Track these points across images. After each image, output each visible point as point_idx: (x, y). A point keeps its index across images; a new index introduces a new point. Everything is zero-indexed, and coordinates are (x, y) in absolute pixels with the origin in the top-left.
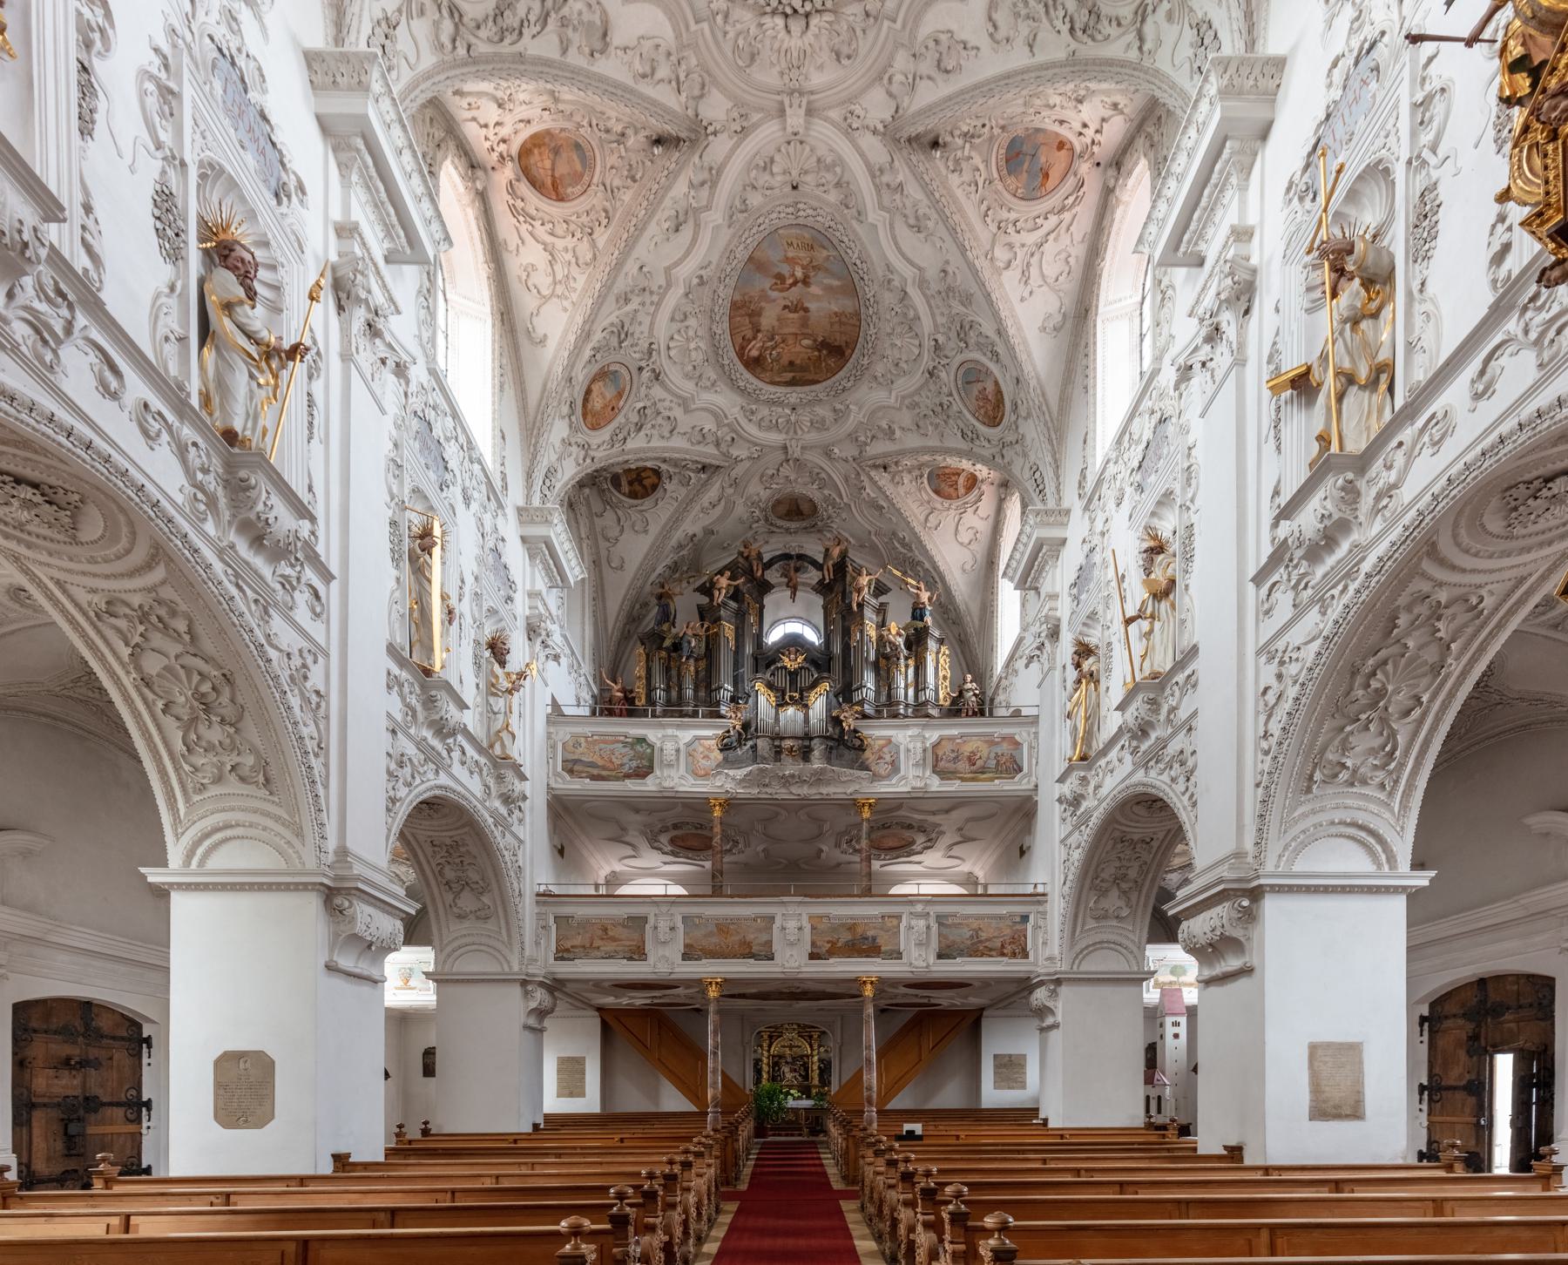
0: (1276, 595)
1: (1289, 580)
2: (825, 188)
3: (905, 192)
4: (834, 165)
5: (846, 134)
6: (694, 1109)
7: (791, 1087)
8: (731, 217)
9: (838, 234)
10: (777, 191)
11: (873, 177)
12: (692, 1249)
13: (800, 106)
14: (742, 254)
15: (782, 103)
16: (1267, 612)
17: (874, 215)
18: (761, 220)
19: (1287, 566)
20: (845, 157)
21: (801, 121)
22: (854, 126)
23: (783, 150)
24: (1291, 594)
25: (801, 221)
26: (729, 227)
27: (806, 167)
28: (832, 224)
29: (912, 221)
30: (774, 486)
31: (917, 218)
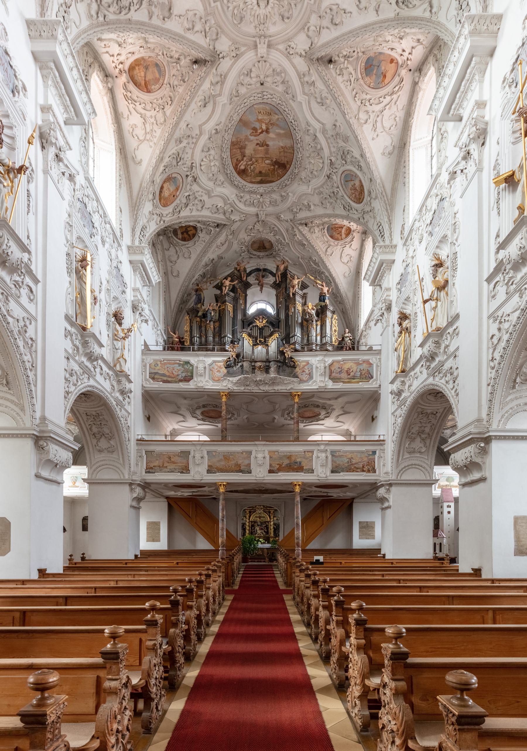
2: (276, 84)
3: (316, 86)
4: (281, 72)
5: (287, 57)
6: (212, 548)
7: (260, 537)
8: (231, 99)
9: (283, 107)
10: (253, 86)
11: (300, 78)
12: (210, 618)
13: (264, 43)
14: (236, 118)
15: (256, 42)
17: (300, 97)
18: (245, 101)
20: (288, 70)
21: (265, 51)
22: (291, 53)
23: (256, 65)
25: (265, 101)
26: (230, 104)
27: (267, 74)
28: (280, 102)
29: (319, 100)
30: (252, 234)
31: (322, 99)
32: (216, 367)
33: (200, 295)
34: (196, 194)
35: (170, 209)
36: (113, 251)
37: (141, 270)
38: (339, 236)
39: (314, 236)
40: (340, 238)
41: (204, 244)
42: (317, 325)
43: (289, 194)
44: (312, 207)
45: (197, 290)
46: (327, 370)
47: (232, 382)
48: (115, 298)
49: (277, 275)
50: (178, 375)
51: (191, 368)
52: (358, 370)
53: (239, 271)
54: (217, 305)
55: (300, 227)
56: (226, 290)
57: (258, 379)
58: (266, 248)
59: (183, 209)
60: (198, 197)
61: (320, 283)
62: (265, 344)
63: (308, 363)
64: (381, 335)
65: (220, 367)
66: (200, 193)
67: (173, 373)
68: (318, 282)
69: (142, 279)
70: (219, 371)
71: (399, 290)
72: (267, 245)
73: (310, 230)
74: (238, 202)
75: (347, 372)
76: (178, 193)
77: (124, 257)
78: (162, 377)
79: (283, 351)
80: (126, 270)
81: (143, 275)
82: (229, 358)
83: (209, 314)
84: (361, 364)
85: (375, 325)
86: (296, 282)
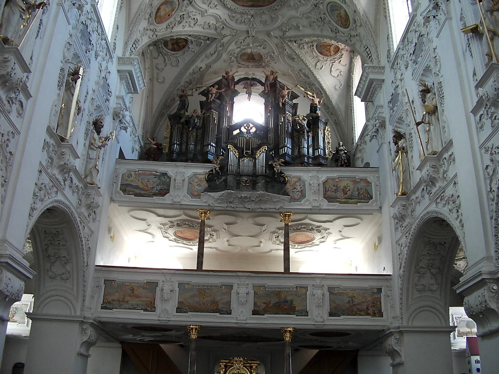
0: (483, 120)
1: (488, 114)
16: (481, 127)
19: (485, 108)
24: (490, 120)
30: (242, 47)
32: (196, 180)
33: (185, 101)
34: (191, 14)
35: (164, 25)
36: (104, 64)
37: (127, 78)
38: (328, 52)
39: (303, 51)
40: (329, 54)
41: (193, 54)
42: (308, 136)
43: (279, 16)
44: (301, 28)
45: (181, 97)
46: (322, 186)
47: (213, 198)
48: (98, 107)
49: (266, 85)
50: (152, 188)
51: (168, 180)
52: (356, 189)
53: (227, 79)
54: (202, 112)
55: (289, 44)
56: (212, 98)
57: (243, 195)
58: (255, 59)
59: (176, 26)
60: (191, 16)
61: (311, 94)
62: (253, 156)
63: (300, 179)
64: (378, 152)
65: (201, 180)
66: (194, 13)
67: (147, 186)
68: (309, 93)
69: (127, 87)
70: (199, 185)
71: (392, 109)
72: (256, 57)
73: (299, 46)
74: (230, 20)
75: (343, 190)
76: (173, 13)
77: (113, 67)
78: (134, 190)
79: (272, 164)
80: (114, 80)
81: (129, 83)
82: (212, 171)
83: (192, 121)
84: (358, 182)
85: (370, 141)
86: (286, 92)
